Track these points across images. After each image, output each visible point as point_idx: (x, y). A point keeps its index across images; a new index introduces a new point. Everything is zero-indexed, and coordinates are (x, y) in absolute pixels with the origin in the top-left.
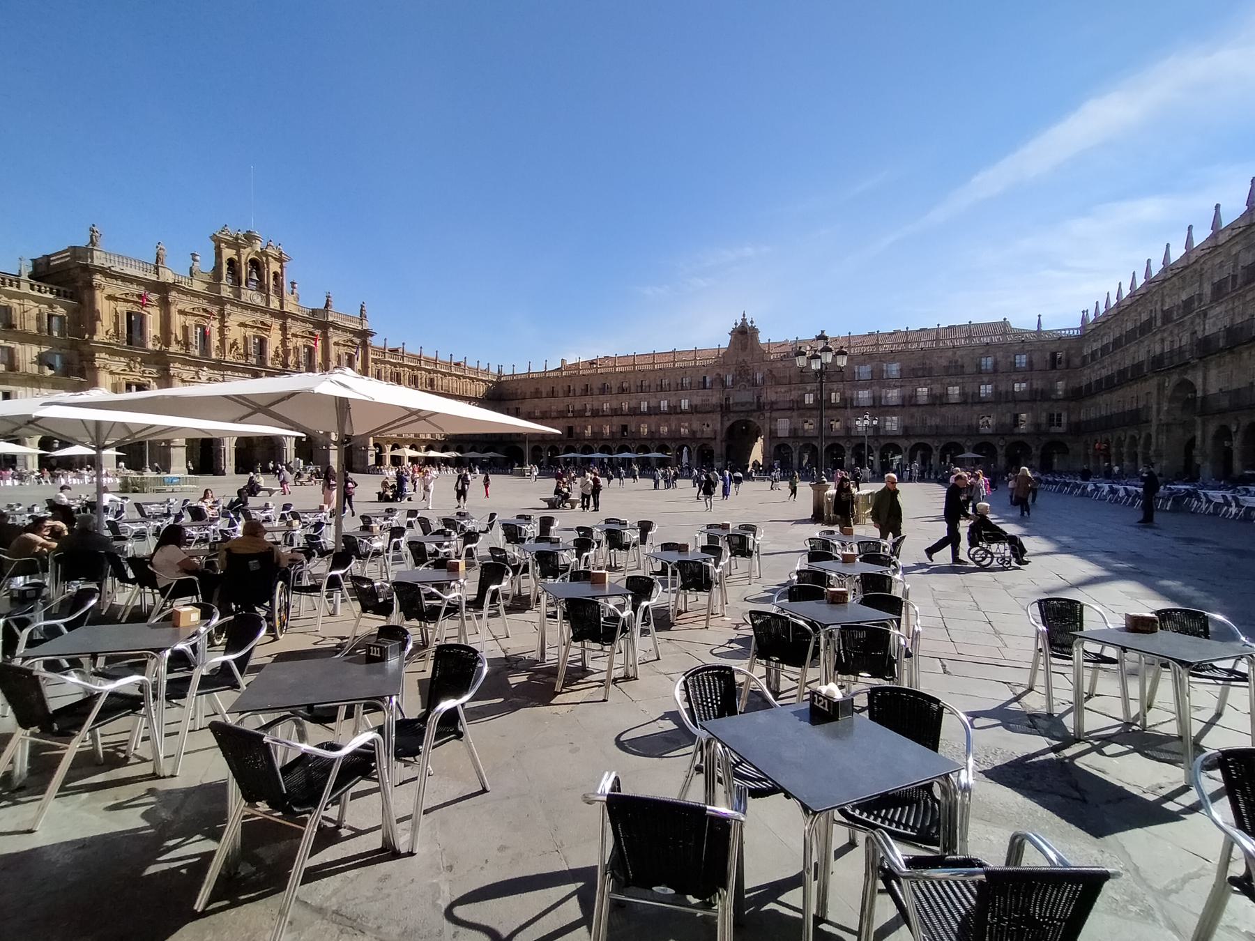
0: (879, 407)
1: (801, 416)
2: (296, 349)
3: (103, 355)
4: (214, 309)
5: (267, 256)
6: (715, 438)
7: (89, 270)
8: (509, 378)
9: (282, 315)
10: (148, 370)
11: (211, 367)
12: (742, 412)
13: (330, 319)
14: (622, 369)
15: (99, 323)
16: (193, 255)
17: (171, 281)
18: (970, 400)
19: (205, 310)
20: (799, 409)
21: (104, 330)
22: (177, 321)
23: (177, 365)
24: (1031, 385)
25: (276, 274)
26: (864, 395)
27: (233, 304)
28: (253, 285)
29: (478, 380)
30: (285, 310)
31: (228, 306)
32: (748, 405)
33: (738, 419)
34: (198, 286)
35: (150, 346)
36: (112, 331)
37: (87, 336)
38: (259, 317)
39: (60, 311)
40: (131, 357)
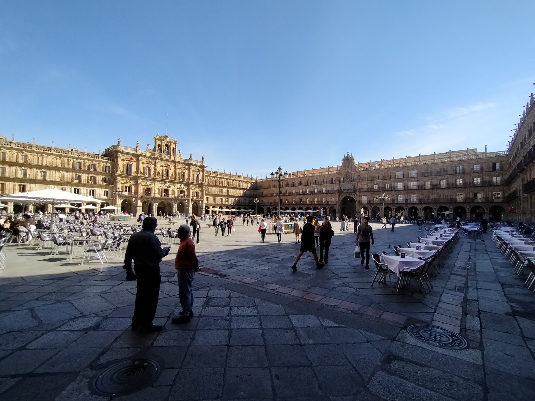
0: (407, 190)
1: (372, 195)
2: (179, 173)
3: (119, 178)
4: (153, 162)
5: (171, 143)
6: (336, 204)
7: (117, 152)
8: (259, 181)
9: (175, 162)
10: (132, 182)
11: (151, 180)
12: (347, 193)
13: (191, 162)
14: (300, 176)
15: (118, 168)
16: (148, 144)
17: (140, 153)
18: (451, 186)
19: (150, 162)
20: (371, 191)
21: (120, 170)
22: (141, 166)
23: (140, 180)
24: (483, 178)
25: (173, 148)
26: (400, 186)
27: (159, 159)
28: (166, 152)
29: (247, 182)
30: (176, 160)
31: (157, 160)
32: (350, 190)
33: (345, 196)
34: (149, 154)
35: (133, 174)
36: (122, 170)
37: (115, 172)
38: (167, 163)
39: (109, 165)
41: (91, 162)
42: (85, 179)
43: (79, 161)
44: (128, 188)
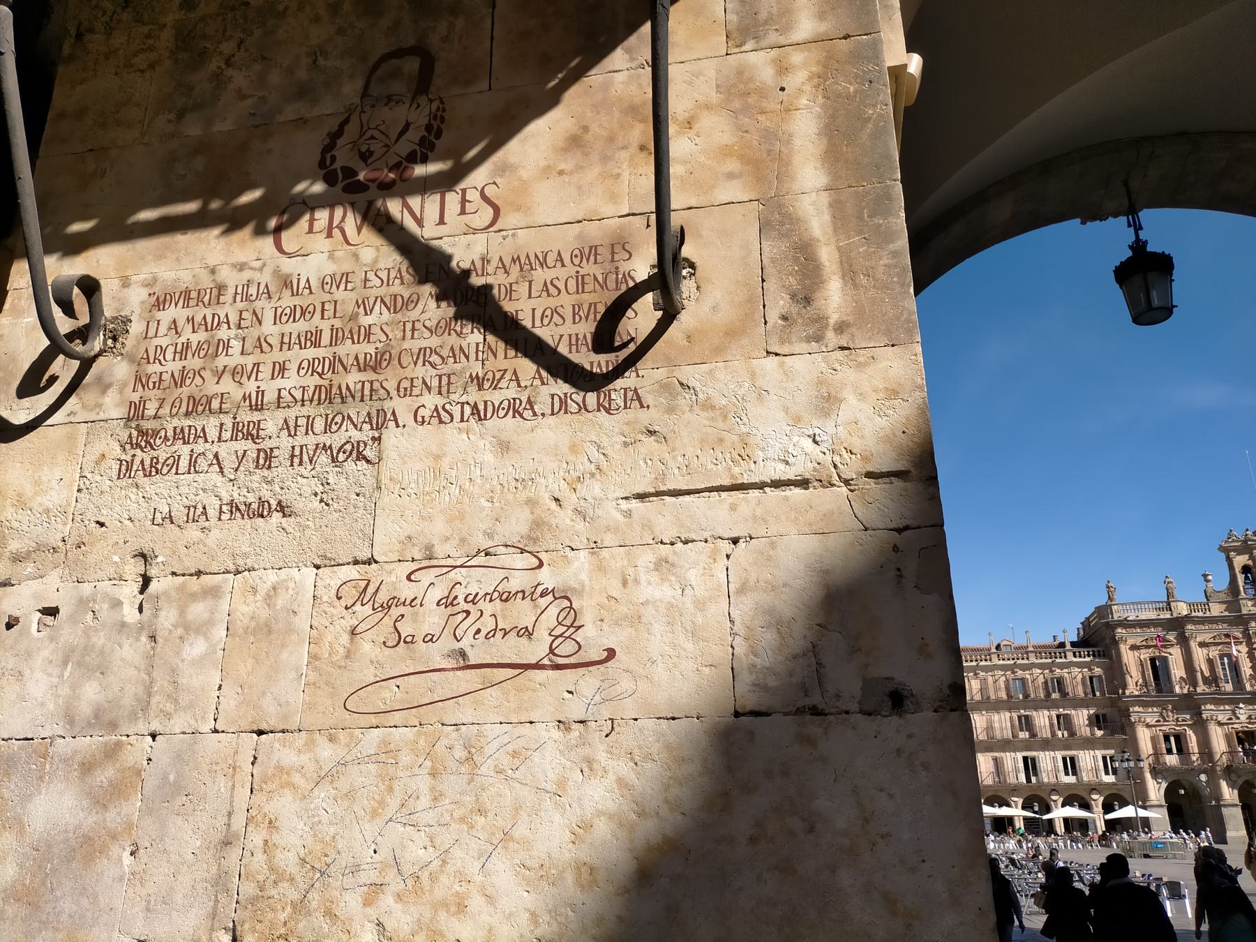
3: (1137, 709)
10: (1181, 717)
11: (1246, 702)
15: (1128, 677)
16: (1205, 576)
17: (1185, 613)
22: (1199, 655)
23: (1209, 707)
34: (1216, 610)
35: (1177, 690)
36: (1141, 681)
37: (1120, 691)
39: (1098, 671)
40: (1162, 706)
41: (1009, 673)
42: (1042, 724)
43: (1020, 673)
44: (1172, 739)
